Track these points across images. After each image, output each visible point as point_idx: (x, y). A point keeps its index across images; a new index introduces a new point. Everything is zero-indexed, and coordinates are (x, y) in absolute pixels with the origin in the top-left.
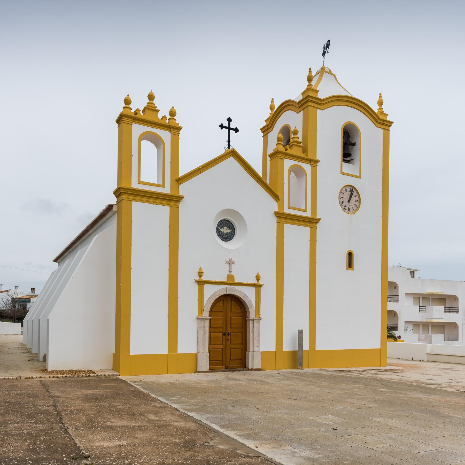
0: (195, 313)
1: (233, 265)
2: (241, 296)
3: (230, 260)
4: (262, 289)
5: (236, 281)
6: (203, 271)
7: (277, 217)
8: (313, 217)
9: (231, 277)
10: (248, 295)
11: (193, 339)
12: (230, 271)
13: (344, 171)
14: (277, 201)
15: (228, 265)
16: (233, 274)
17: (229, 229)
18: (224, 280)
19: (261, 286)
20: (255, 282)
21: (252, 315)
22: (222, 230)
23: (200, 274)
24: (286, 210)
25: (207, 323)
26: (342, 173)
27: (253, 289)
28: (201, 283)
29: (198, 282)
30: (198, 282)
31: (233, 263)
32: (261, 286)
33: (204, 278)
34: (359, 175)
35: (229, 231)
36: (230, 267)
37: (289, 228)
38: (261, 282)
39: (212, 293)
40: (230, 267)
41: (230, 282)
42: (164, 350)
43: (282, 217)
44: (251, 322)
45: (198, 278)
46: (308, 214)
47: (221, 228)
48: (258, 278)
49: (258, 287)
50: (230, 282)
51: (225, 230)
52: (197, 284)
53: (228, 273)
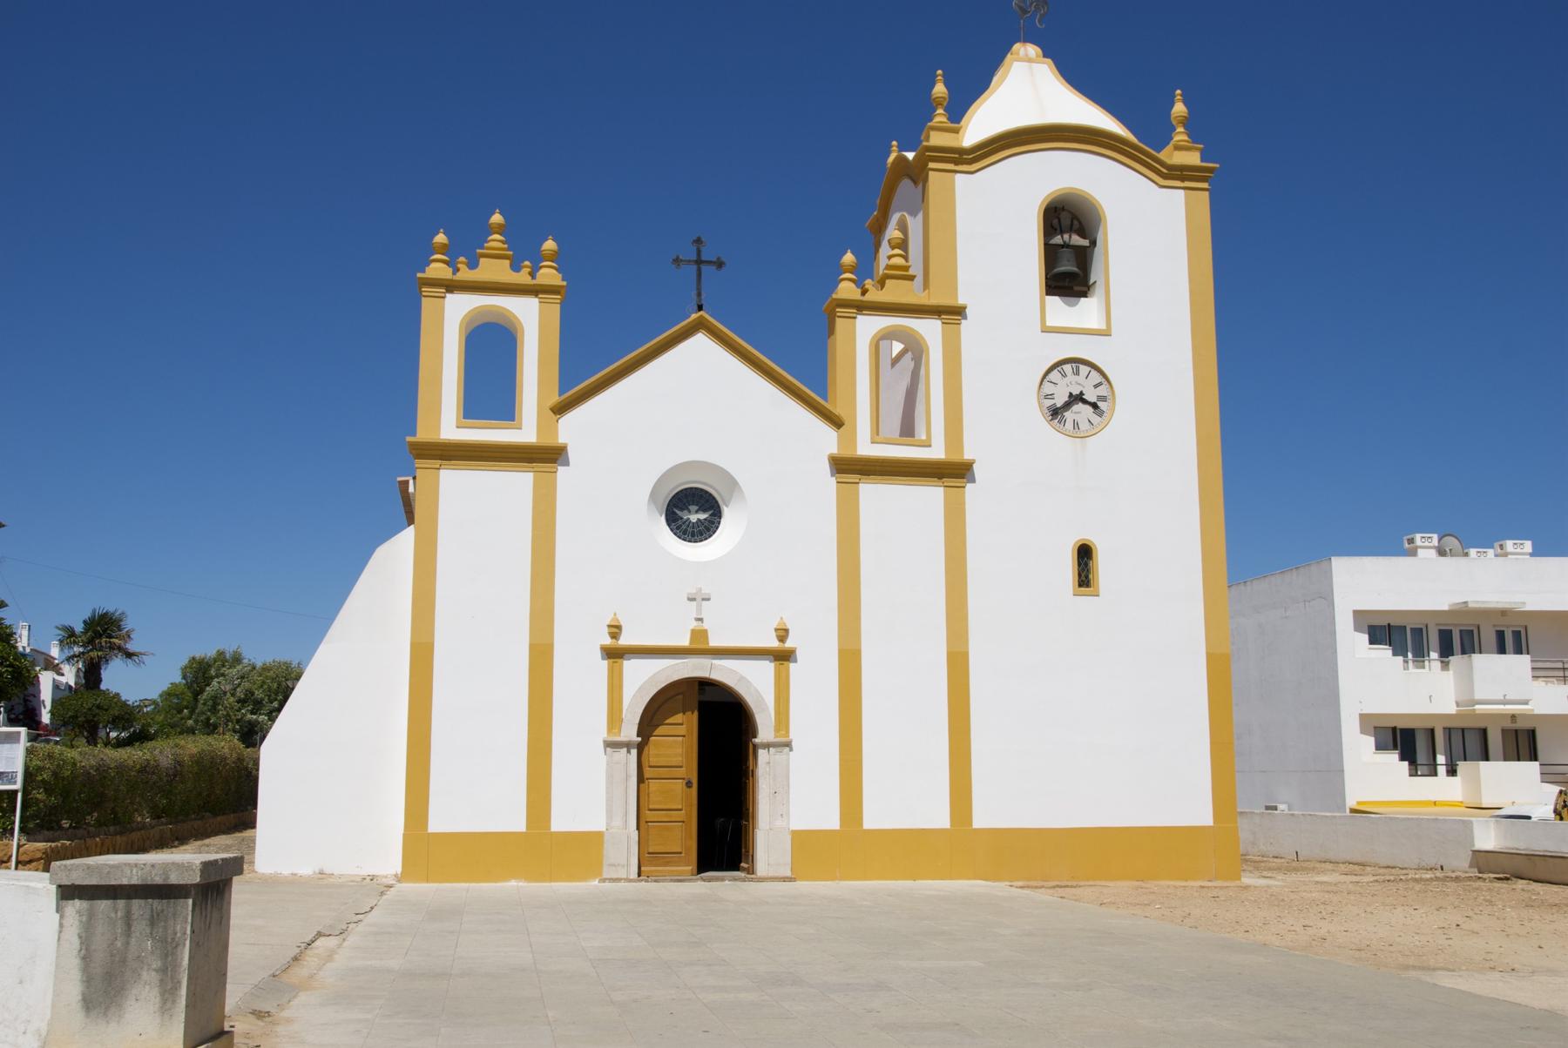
0: (603, 733)
5: (714, 642)
8: (955, 458)
9: (699, 635)
10: (752, 682)
11: (594, 792)
13: (1049, 323)
16: (705, 625)
17: (705, 511)
18: (684, 641)
20: (773, 643)
23: (615, 630)
24: (866, 448)
26: (1046, 330)
27: (767, 668)
28: (614, 654)
33: (625, 641)
34: (1104, 327)
35: (703, 516)
36: (699, 609)
37: (872, 493)
38: (789, 644)
39: (642, 679)
40: (699, 609)
41: (699, 648)
42: (515, 821)
43: (848, 468)
45: (608, 641)
48: (783, 634)
49: (783, 657)
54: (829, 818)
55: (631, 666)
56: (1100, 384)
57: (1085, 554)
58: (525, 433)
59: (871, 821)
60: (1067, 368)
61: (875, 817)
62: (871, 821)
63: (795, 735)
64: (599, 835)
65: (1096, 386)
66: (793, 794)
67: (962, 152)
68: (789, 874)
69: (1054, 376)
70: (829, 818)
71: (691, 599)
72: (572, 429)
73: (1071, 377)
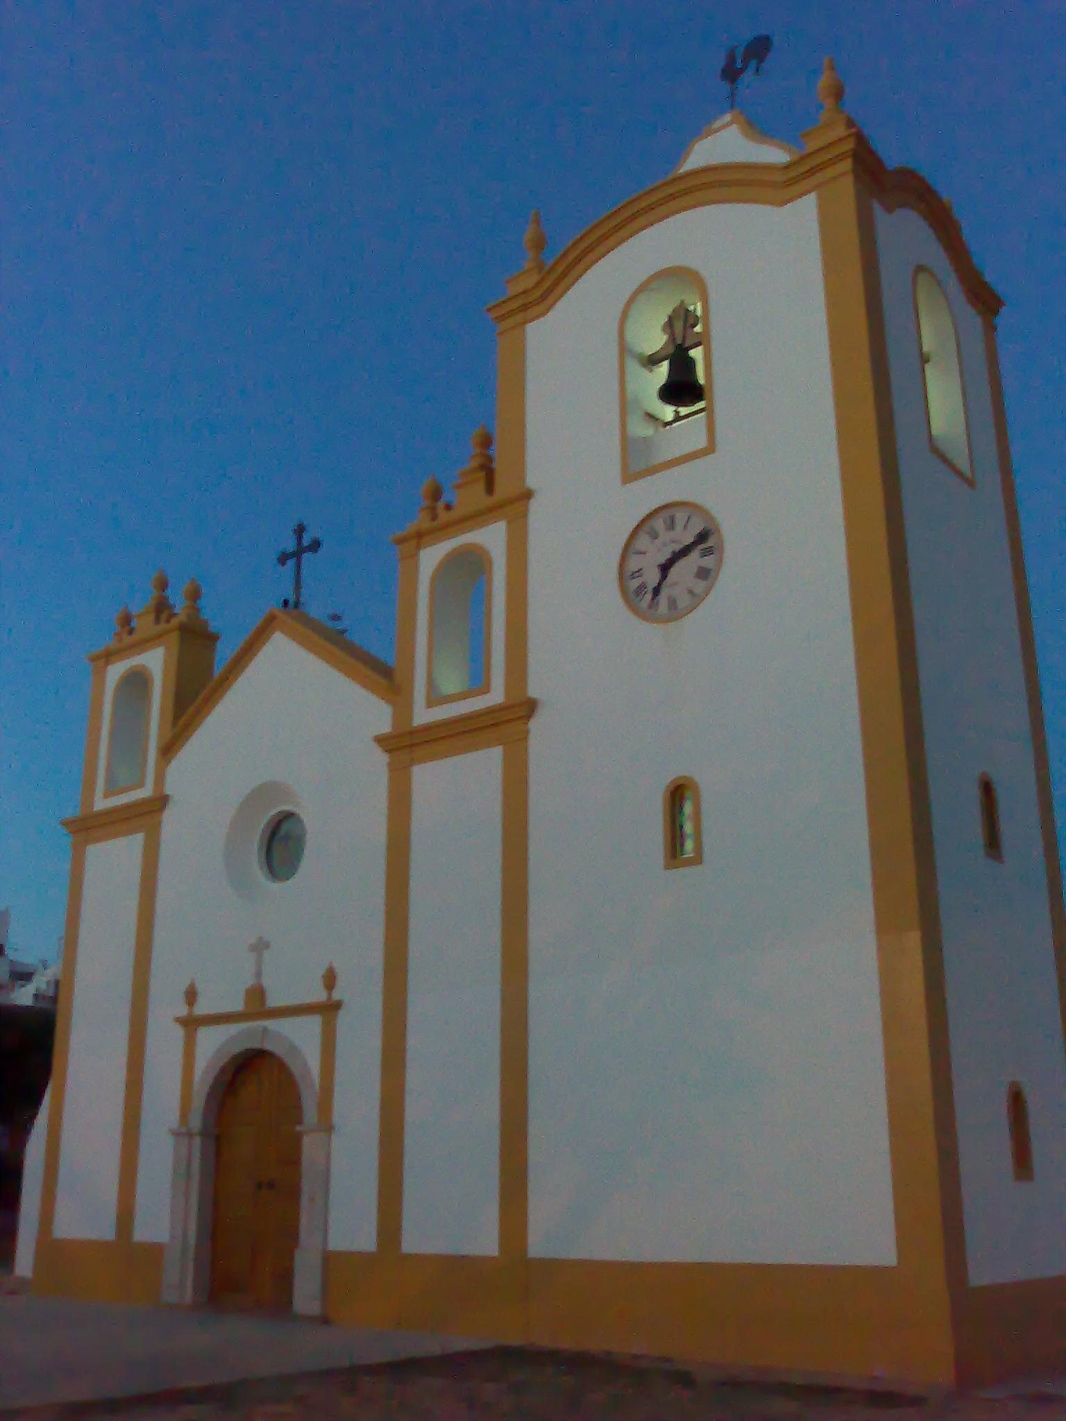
6: (200, 987)
9: (257, 994)
12: (258, 974)
20: (320, 996)
21: (310, 1115)
23: (191, 996)
27: (313, 1024)
28: (191, 1024)
38: (336, 995)
44: (306, 1140)
45: (183, 1011)
48: (330, 980)
49: (329, 1009)
59: (412, 1243)
60: (659, 524)
61: (419, 1238)
62: (412, 1243)
69: (643, 542)
73: (665, 536)
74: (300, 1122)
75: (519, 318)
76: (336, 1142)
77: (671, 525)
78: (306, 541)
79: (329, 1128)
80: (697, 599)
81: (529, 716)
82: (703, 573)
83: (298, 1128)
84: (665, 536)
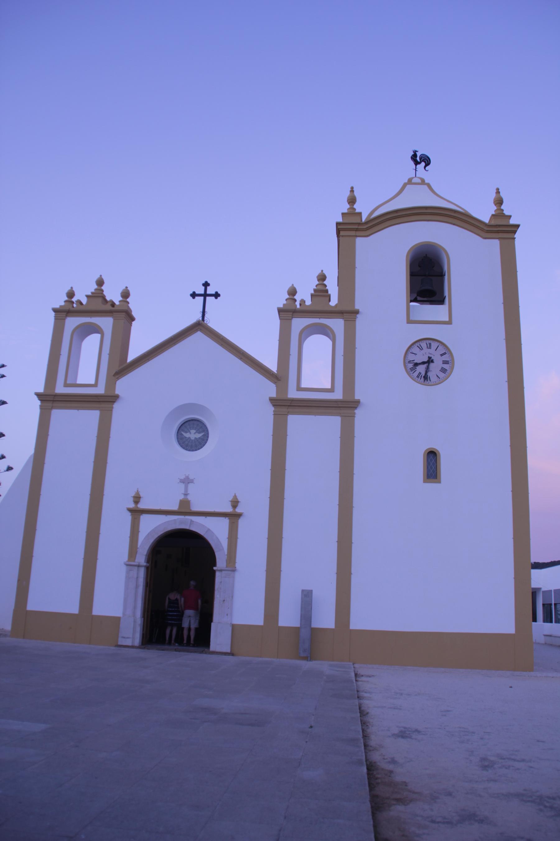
0: (125, 557)
1: (190, 486)
2: (201, 532)
3: (187, 478)
4: (241, 521)
5: (195, 508)
6: (142, 494)
7: (274, 405)
12: (186, 495)
13: (412, 318)
14: (275, 383)
15: (182, 486)
17: (199, 433)
18: (175, 508)
19: (239, 515)
20: (229, 509)
21: (221, 562)
22: (187, 435)
23: (137, 499)
24: (293, 394)
25: (142, 572)
26: (409, 321)
27: (225, 522)
28: (136, 513)
29: (130, 510)
30: (130, 510)
31: (192, 481)
32: (239, 515)
33: (141, 506)
34: (447, 319)
36: (186, 489)
37: (295, 422)
38: (238, 510)
40: (186, 489)
41: (185, 509)
43: (284, 406)
44: (218, 574)
45: (132, 505)
46: (338, 395)
47: (186, 432)
48: (235, 503)
49: (234, 517)
50: (185, 509)
51: (193, 435)
52: (129, 514)
53: (182, 497)
54: (256, 617)
55: (145, 519)
56: (445, 354)
57: (432, 456)
58: (100, 390)
60: (424, 344)
63: (237, 566)
64: (119, 618)
65: (442, 355)
66: (240, 601)
67: (359, 224)
68: (229, 651)
70: (256, 617)
71: (182, 481)
72: (122, 386)
73: (425, 350)
74: (215, 565)
75: (353, 233)
76: (237, 575)
77: (429, 347)
78: (210, 291)
79: (234, 570)
80: (440, 381)
81: (356, 408)
82: (443, 370)
83: (215, 568)
84: (432, 351)
